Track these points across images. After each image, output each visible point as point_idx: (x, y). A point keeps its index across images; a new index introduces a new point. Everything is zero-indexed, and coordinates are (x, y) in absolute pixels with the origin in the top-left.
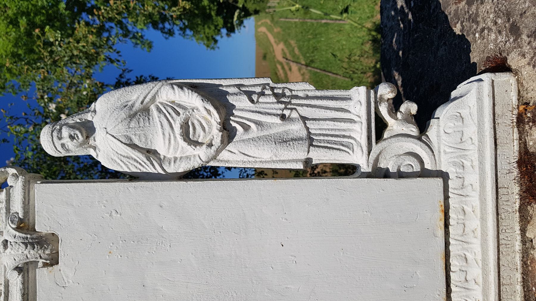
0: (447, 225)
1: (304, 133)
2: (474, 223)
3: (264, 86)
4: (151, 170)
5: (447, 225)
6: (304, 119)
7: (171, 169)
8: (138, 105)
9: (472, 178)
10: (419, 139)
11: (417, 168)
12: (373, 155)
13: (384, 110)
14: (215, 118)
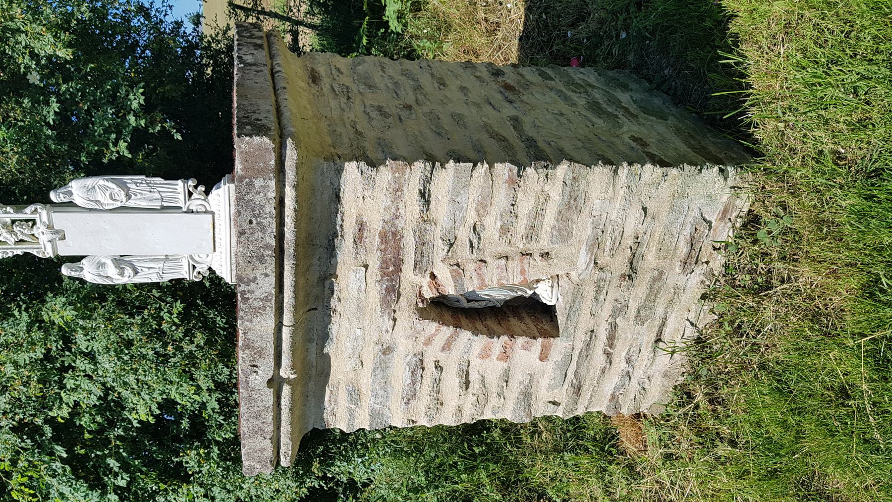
0: (214, 228)
1: (160, 197)
2: (223, 227)
3: (142, 180)
4: (98, 208)
5: (214, 228)
6: (159, 192)
7: (107, 208)
8: (90, 186)
9: (222, 214)
10: (205, 200)
11: (204, 210)
12: (187, 205)
13: (191, 189)
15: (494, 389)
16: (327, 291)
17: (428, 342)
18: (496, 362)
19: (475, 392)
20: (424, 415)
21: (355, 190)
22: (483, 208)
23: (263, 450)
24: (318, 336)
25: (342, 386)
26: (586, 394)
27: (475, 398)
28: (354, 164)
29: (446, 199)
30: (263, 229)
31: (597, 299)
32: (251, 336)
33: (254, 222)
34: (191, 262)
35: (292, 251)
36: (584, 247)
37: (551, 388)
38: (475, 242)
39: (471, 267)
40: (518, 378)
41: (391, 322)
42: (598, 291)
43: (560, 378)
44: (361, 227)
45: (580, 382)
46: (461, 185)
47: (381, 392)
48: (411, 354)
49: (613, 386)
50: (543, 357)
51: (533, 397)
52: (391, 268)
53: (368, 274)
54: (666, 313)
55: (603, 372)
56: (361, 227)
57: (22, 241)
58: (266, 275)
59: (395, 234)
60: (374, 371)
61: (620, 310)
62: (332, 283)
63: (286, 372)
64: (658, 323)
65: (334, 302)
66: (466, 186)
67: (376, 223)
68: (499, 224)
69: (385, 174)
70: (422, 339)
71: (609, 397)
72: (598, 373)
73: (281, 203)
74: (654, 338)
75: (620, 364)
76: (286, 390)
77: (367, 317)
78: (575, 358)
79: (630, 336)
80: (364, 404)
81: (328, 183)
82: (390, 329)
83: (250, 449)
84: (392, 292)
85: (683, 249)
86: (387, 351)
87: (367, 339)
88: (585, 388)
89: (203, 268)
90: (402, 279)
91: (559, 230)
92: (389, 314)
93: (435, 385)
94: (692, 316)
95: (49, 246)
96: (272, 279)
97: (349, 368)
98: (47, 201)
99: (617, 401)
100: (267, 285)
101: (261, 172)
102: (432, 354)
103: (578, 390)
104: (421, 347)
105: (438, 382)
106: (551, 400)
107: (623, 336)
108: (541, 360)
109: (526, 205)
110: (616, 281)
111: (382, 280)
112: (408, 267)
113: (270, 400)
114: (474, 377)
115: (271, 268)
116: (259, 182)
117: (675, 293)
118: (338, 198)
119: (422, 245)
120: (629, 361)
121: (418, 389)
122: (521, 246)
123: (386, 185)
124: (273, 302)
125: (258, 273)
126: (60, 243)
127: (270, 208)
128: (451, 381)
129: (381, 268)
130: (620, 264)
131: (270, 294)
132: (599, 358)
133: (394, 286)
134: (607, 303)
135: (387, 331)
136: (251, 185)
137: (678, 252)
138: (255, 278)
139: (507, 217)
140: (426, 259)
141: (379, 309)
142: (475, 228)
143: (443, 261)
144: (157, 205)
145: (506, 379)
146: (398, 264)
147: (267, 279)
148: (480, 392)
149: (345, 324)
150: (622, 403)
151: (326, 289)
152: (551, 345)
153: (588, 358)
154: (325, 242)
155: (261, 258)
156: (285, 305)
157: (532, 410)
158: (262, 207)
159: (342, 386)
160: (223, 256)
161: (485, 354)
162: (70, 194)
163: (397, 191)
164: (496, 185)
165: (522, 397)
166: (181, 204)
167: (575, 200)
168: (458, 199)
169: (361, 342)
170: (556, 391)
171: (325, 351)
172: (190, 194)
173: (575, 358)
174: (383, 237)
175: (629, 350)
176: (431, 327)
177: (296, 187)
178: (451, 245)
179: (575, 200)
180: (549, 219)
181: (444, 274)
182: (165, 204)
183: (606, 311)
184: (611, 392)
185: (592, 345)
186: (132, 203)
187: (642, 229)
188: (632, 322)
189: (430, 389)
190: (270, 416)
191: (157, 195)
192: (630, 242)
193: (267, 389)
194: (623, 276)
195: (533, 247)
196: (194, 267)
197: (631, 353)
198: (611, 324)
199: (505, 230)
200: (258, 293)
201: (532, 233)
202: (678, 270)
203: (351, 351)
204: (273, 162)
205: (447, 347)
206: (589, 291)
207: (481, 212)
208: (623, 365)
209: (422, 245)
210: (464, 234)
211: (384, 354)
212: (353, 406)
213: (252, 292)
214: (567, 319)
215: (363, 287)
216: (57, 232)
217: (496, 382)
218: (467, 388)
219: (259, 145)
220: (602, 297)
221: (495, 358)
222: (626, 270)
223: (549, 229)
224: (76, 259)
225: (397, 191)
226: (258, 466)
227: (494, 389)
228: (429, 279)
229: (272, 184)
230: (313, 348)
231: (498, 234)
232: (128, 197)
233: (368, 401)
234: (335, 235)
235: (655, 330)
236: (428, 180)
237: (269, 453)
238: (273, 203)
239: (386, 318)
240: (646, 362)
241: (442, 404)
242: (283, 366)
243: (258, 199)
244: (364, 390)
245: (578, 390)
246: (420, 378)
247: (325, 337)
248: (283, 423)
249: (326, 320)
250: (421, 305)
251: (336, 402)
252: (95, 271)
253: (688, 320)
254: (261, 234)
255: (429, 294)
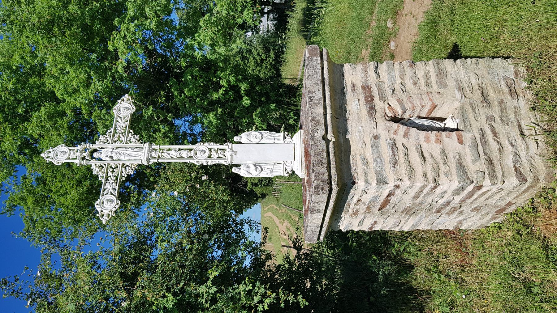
14: (260, 135)
15: (441, 162)
16: (344, 112)
17: (395, 133)
18: (435, 144)
19: (430, 163)
20: (405, 175)
21: (349, 72)
22: (402, 76)
23: (323, 174)
24: (343, 132)
25: (358, 156)
26: (498, 168)
27: (431, 166)
28: (347, 64)
29: (386, 74)
30: (317, 74)
31: (475, 112)
32: (314, 115)
33: (313, 71)
34: (285, 166)
35: (328, 82)
36: (456, 90)
37: (474, 162)
38: (404, 89)
39: (405, 99)
40: (451, 155)
41: (375, 123)
42: (473, 108)
43: (476, 155)
44: (354, 85)
45: (489, 158)
46: (391, 68)
47: (378, 160)
48: (388, 140)
49: (512, 161)
50: (461, 142)
51: (466, 168)
52: (369, 99)
53: (360, 102)
54: (517, 119)
55: (500, 152)
56: (354, 85)
57: (220, 157)
58: (319, 90)
59: (368, 86)
60: (372, 147)
61: (490, 119)
62: (345, 107)
63: (330, 136)
64: (515, 124)
65: (347, 115)
66: (393, 69)
67: (359, 84)
68: (412, 81)
69: (359, 67)
70: (392, 132)
71: (513, 169)
72: (498, 153)
73: (322, 68)
74: (519, 132)
75: (508, 148)
76: (331, 144)
77: (363, 122)
78: (479, 143)
79: (504, 132)
80: (371, 167)
81: (339, 70)
82: (375, 127)
83: (317, 172)
84: (372, 110)
85: (506, 90)
86: (376, 137)
87: (365, 132)
88: (495, 162)
89: (289, 169)
90: (375, 104)
91: (440, 82)
92: (373, 120)
93: (406, 157)
94: (533, 121)
95: (230, 157)
96: (321, 92)
97: (359, 146)
98: (232, 142)
99: (521, 173)
100: (320, 94)
101: (316, 55)
102: (400, 140)
103: (491, 162)
104: (392, 136)
105: (407, 155)
106: (478, 170)
107: (501, 132)
108: (460, 143)
109: (421, 74)
110: (480, 105)
111: (366, 104)
112: (376, 99)
113: (325, 148)
114: (426, 155)
115: (321, 88)
116: (314, 58)
117: (515, 108)
118: (343, 75)
119: (380, 90)
120: (511, 144)
121: (397, 159)
122: (425, 89)
123: (360, 70)
124: (322, 101)
125: (316, 89)
126: (234, 156)
127: (319, 67)
128: (415, 157)
129: (365, 99)
130: (477, 97)
131: (321, 98)
132: (494, 145)
133: (372, 106)
134: (481, 115)
135: (374, 128)
136: (312, 59)
137: (505, 91)
138: (315, 91)
139: (414, 78)
140: (384, 95)
141: (367, 117)
142: (401, 83)
143: (392, 97)
144: (272, 141)
145: (444, 152)
146: (372, 99)
147: (319, 92)
148: (433, 162)
149: (354, 125)
150: (524, 174)
151: (343, 110)
152: (461, 135)
153: (487, 144)
154: (340, 92)
155: (316, 84)
156: (327, 104)
157: (469, 176)
158: (316, 66)
159: (358, 156)
160: (298, 161)
161: (427, 140)
162: (241, 137)
163: (365, 71)
164: (405, 69)
165: (458, 165)
166: (282, 142)
167: (442, 70)
168: (391, 74)
169: (363, 133)
170: (478, 163)
171: (347, 137)
172: (285, 138)
173: (479, 143)
174: (363, 87)
175: (508, 139)
176: (395, 126)
177: (327, 61)
178: (393, 91)
179: (442, 70)
180: (433, 78)
181: (394, 103)
182: (276, 141)
183: (483, 119)
184: (512, 165)
185: (485, 136)
186: (263, 141)
187: (480, 83)
188: (501, 124)
189: (404, 159)
190: (325, 155)
191: (273, 137)
192: (477, 87)
193: (322, 140)
194: (482, 102)
195: (430, 90)
196: (286, 170)
197: (510, 140)
198: (489, 124)
199: (415, 83)
200: (316, 98)
201: (428, 84)
202: (510, 98)
203: (359, 138)
204: (319, 52)
205: (406, 135)
206: (468, 108)
207: (402, 77)
208: (510, 147)
209: (380, 90)
210: (398, 87)
211: (375, 139)
212: (365, 168)
213: (314, 97)
214: (464, 123)
215: (359, 108)
216: (234, 152)
217: (440, 157)
218: (425, 161)
219: (314, 47)
220: (477, 111)
221: (434, 143)
222: (482, 98)
223: (435, 83)
224: (238, 166)
225: (365, 71)
226: (321, 184)
227: (441, 162)
228: (388, 105)
229: (319, 58)
230: (341, 137)
231: (412, 85)
232: (262, 138)
233: (372, 165)
234: (344, 88)
235: (517, 127)
236: (377, 68)
237: (326, 176)
238: (320, 65)
239: (372, 121)
240: (523, 146)
241: (413, 169)
242: (329, 133)
243: (314, 63)
244: (369, 160)
245: (491, 162)
246: (397, 153)
247: (346, 131)
248: (332, 161)
249: (345, 123)
250: (387, 118)
251: (357, 166)
252: (245, 168)
253: (531, 122)
254: (316, 76)
255: (390, 114)
